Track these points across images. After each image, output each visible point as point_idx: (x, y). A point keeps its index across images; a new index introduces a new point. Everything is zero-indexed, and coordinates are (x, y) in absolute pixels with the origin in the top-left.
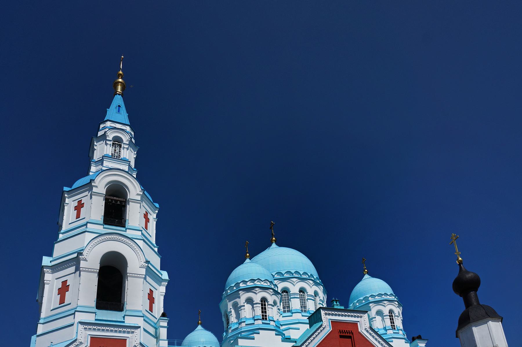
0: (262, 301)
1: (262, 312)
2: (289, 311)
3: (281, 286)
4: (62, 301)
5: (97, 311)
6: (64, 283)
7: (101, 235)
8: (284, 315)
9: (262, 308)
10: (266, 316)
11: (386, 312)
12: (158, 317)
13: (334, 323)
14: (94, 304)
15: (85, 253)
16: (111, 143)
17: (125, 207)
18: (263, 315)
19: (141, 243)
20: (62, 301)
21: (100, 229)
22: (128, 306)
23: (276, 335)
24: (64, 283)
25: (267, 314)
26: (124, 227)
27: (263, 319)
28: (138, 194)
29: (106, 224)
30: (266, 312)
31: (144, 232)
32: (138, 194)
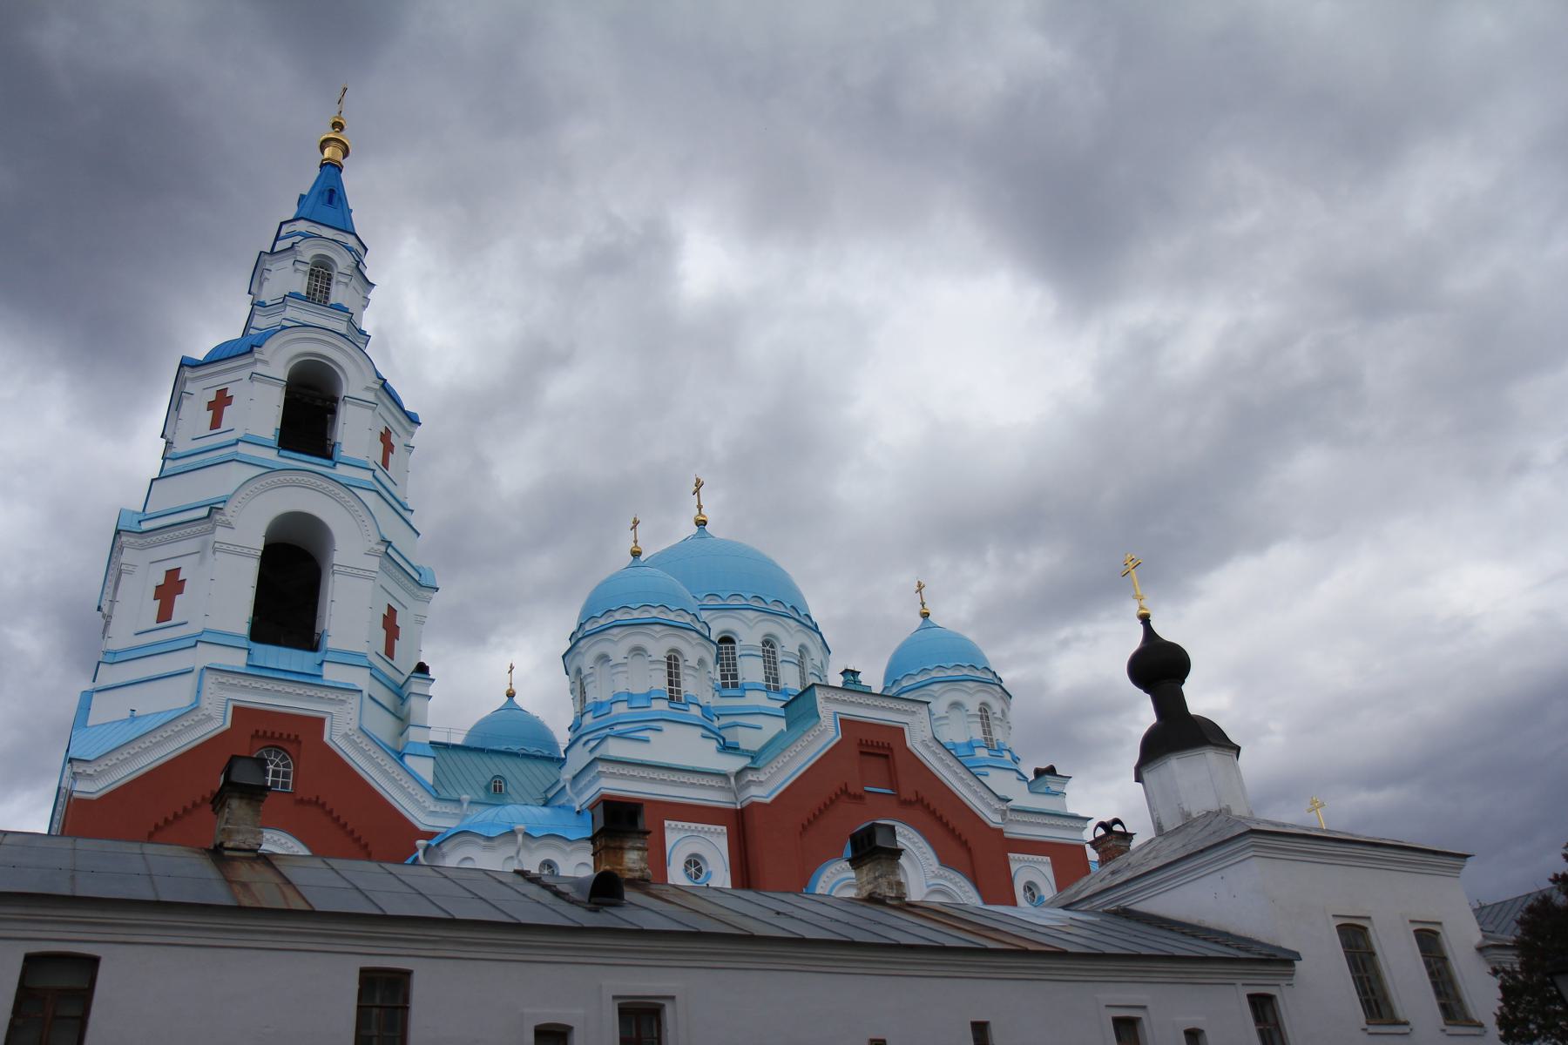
0: (669, 658)
1: (671, 683)
2: (735, 685)
3: (719, 626)
4: (165, 614)
5: (253, 645)
6: (173, 574)
7: (274, 470)
8: (726, 692)
9: (670, 674)
10: (679, 692)
11: (973, 705)
12: (407, 674)
13: (847, 724)
14: (244, 629)
15: (229, 509)
16: (307, 268)
17: (333, 412)
18: (671, 691)
19: (370, 499)
20: (165, 614)
21: (271, 455)
22: (330, 643)
23: (704, 737)
24: (173, 574)
25: (682, 689)
26: (330, 457)
27: (672, 698)
28: (368, 389)
29: (285, 448)
30: (678, 684)
31: (379, 473)
32: (368, 389)
